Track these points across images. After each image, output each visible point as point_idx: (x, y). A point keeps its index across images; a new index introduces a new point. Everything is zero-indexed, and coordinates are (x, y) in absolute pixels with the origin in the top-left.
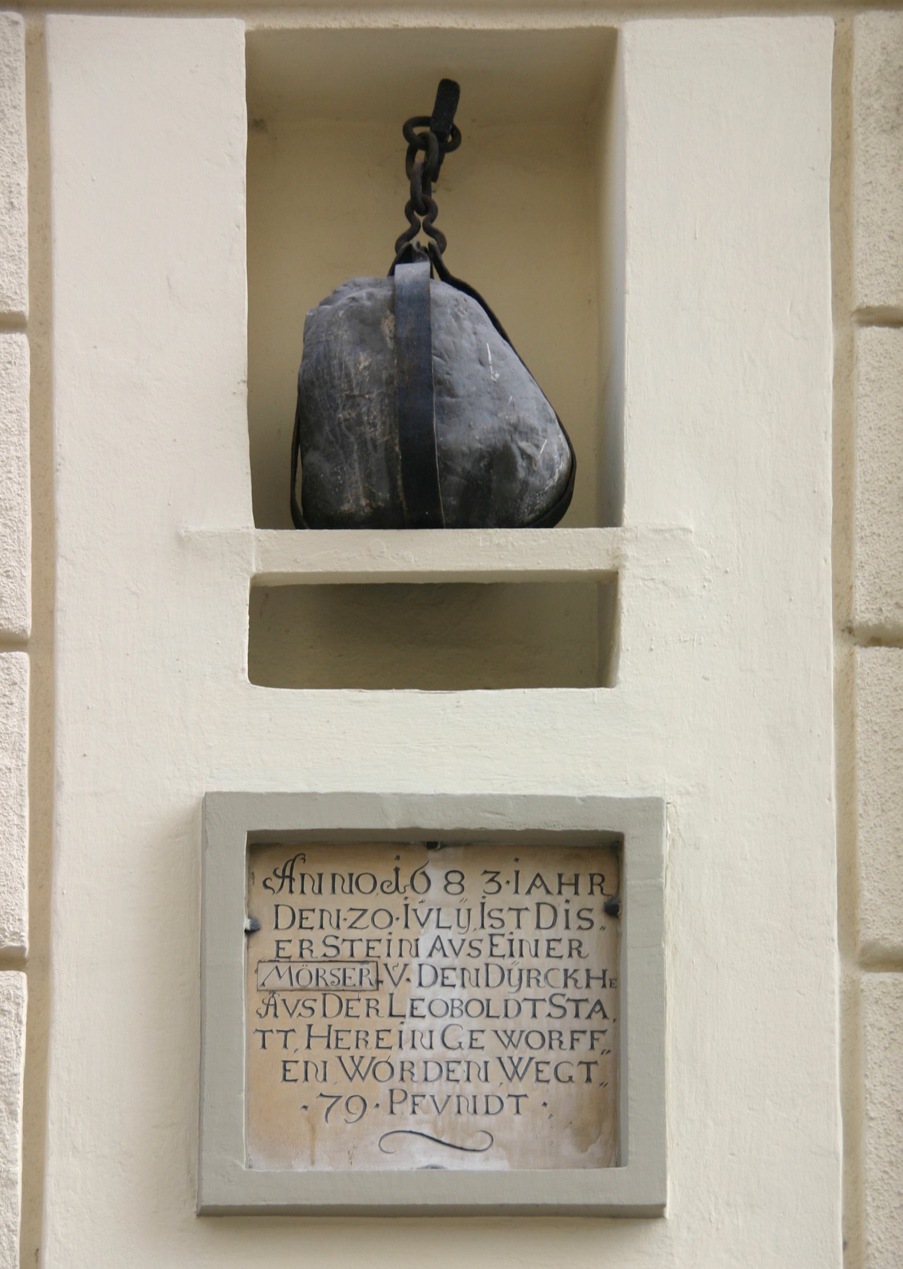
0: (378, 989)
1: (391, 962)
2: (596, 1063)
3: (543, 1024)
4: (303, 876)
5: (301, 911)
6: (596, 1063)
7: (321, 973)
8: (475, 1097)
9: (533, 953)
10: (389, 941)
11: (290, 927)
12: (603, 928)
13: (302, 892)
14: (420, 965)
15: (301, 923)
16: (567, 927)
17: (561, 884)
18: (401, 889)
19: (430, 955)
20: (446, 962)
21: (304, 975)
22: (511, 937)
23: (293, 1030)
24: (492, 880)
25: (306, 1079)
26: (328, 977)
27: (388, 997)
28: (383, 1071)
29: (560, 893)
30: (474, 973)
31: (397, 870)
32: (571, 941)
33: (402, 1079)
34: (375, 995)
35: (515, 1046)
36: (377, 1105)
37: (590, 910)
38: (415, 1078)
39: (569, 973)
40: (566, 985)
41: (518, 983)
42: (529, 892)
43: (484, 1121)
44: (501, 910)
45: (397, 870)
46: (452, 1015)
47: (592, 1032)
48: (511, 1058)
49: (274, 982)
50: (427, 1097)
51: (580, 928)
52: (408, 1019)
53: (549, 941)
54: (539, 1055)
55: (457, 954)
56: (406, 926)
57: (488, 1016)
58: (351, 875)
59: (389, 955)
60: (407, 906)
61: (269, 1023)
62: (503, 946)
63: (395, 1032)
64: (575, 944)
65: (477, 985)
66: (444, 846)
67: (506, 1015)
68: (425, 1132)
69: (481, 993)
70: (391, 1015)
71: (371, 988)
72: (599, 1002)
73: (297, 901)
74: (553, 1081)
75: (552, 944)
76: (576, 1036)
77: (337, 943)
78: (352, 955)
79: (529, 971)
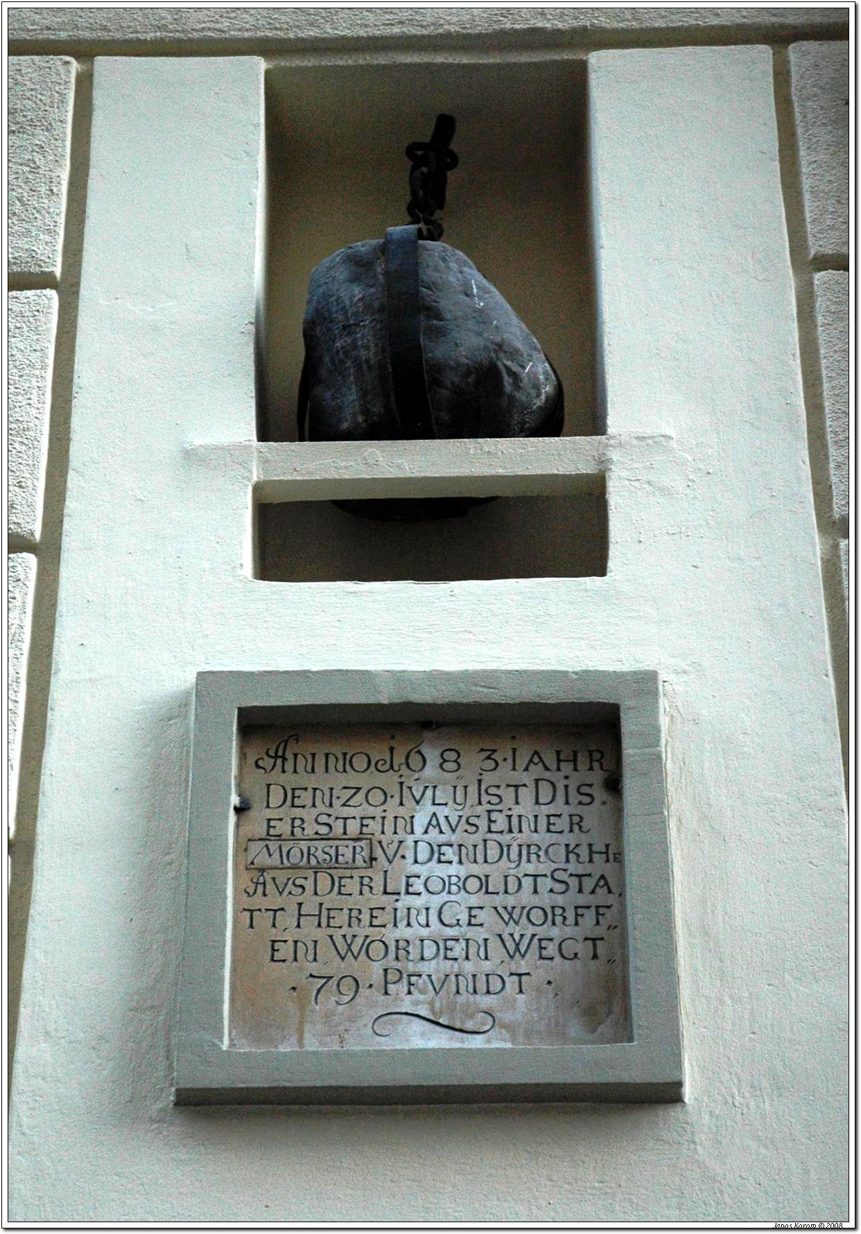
2: (602, 939)
3: (545, 900)
4: (296, 755)
5: (293, 790)
6: (602, 939)
8: (474, 976)
9: (533, 828)
10: (384, 818)
12: (604, 803)
13: (295, 771)
14: (416, 842)
16: (567, 803)
17: (559, 761)
18: (396, 768)
19: (426, 832)
20: (442, 839)
21: (295, 852)
22: (509, 813)
23: (282, 909)
24: (489, 758)
26: (319, 854)
27: (382, 873)
28: (377, 949)
29: (559, 769)
30: (471, 848)
31: (392, 749)
32: (571, 816)
33: (397, 958)
34: (369, 872)
35: (516, 923)
36: (371, 986)
37: (590, 786)
38: (411, 957)
39: (571, 848)
40: (568, 861)
42: (526, 769)
43: (485, 1001)
45: (392, 749)
47: (597, 907)
48: (512, 935)
49: (263, 860)
50: (424, 976)
51: (580, 803)
52: (402, 896)
53: (548, 816)
54: (542, 931)
55: (454, 831)
56: (401, 804)
57: (487, 892)
58: (345, 754)
59: (383, 832)
60: (401, 784)
61: (258, 901)
62: (501, 822)
63: (389, 909)
64: (576, 819)
65: (475, 861)
66: (439, 725)
67: (506, 892)
72: (602, 877)
73: (289, 779)
74: (558, 959)
75: (552, 820)
76: (580, 911)
77: (330, 821)
78: (345, 833)
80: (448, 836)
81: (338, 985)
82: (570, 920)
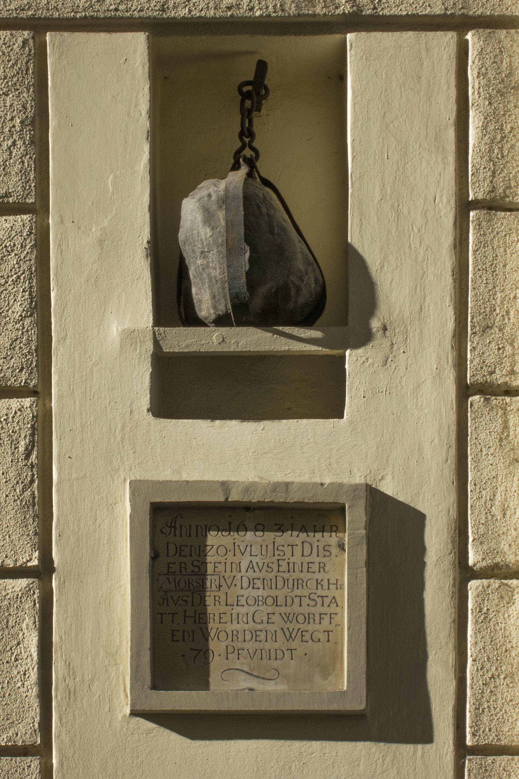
0: (220, 590)
1: (226, 575)
7: (191, 581)
8: (270, 650)
10: (225, 563)
11: (175, 555)
14: (242, 577)
15: (180, 553)
19: (247, 571)
20: (255, 575)
22: (289, 561)
25: (184, 640)
26: (195, 584)
28: (223, 636)
38: (239, 640)
40: (317, 589)
41: (292, 587)
44: (283, 546)
46: (258, 605)
47: (331, 614)
53: (308, 563)
54: (303, 627)
56: (235, 555)
62: (284, 566)
63: (228, 614)
67: (286, 605)
68: (245, 669)
69: (273, 593)
70: (227, 605)
71: (217, 589)
72: (334, 597)
74: (310, 641)
79: (298, 580)
80: (257, 574)
81: (205, 654)
82: (317, 621)
